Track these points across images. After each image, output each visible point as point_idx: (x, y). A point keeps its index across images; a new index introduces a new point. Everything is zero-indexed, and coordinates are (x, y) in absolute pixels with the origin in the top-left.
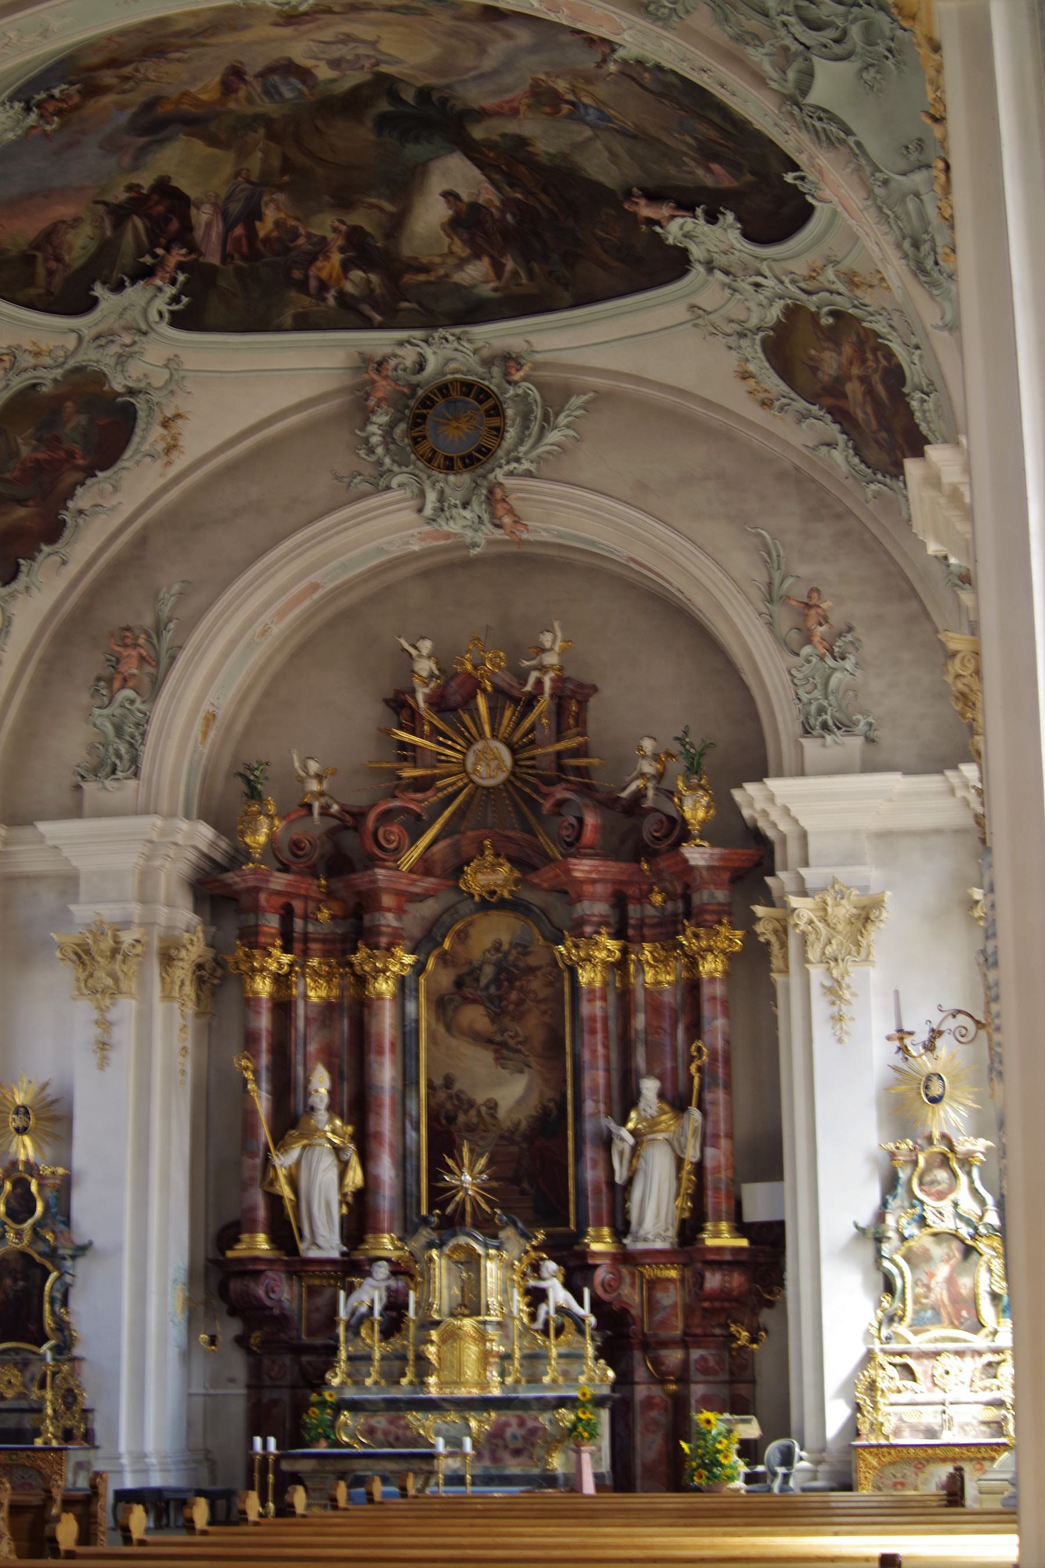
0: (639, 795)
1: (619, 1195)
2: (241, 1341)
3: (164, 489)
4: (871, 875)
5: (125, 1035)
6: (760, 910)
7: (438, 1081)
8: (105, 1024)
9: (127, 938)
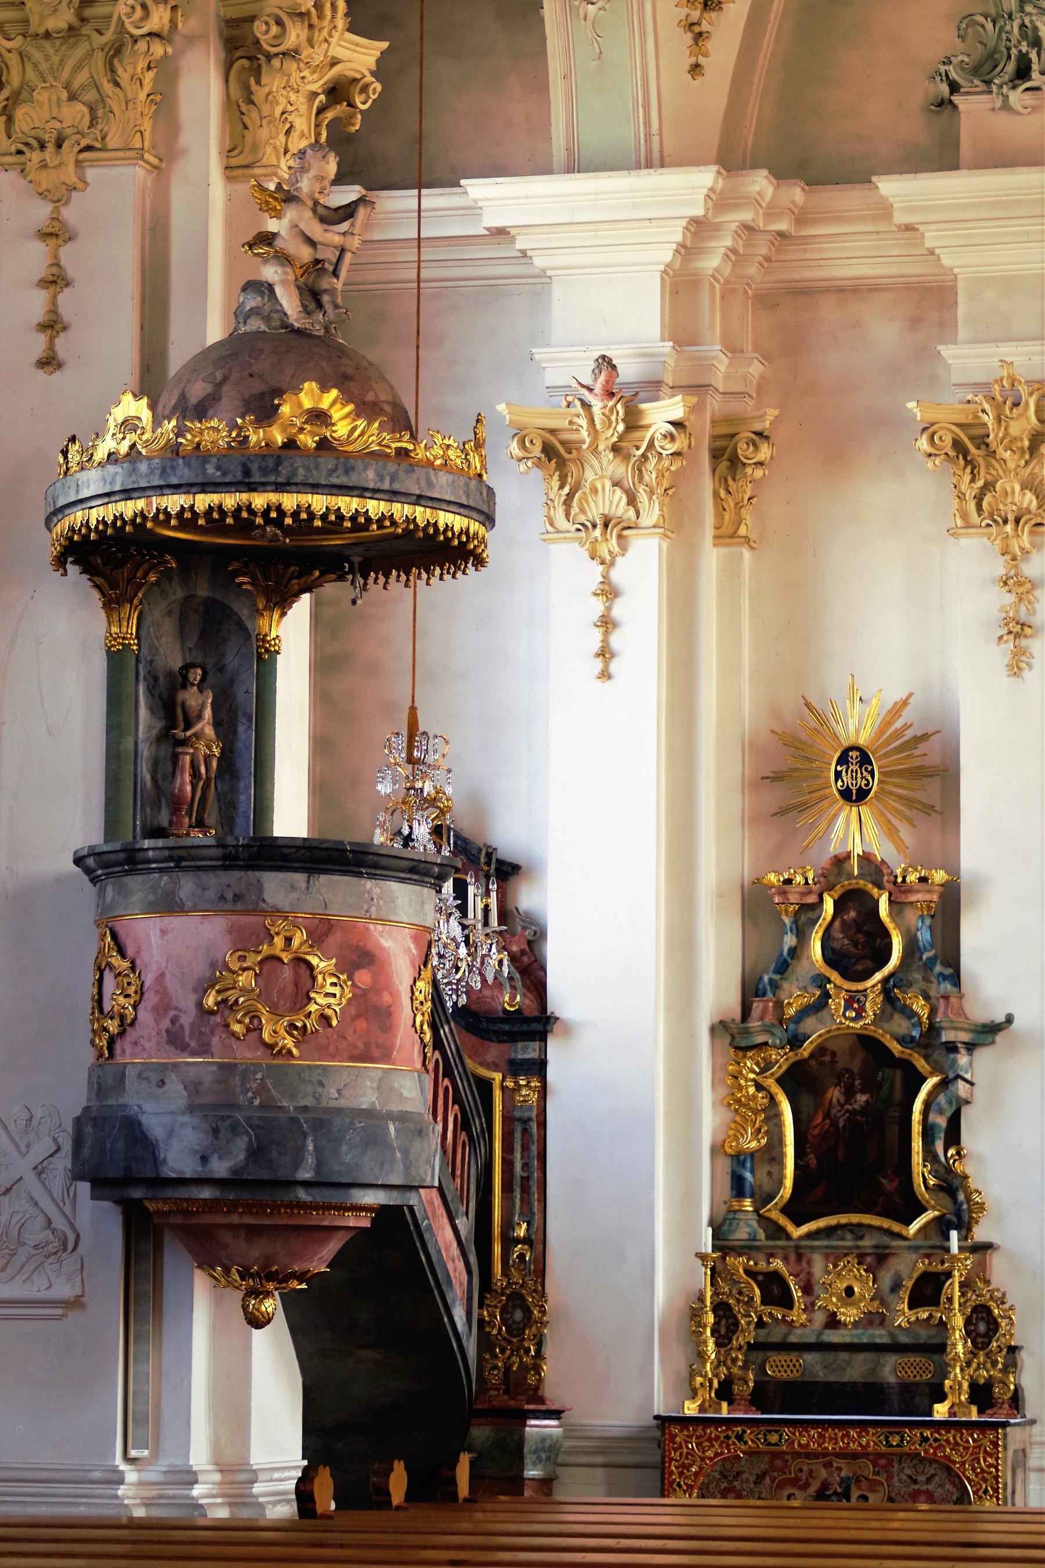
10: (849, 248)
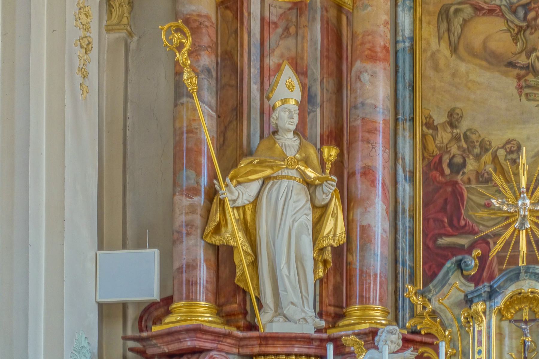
7: (440, 118)
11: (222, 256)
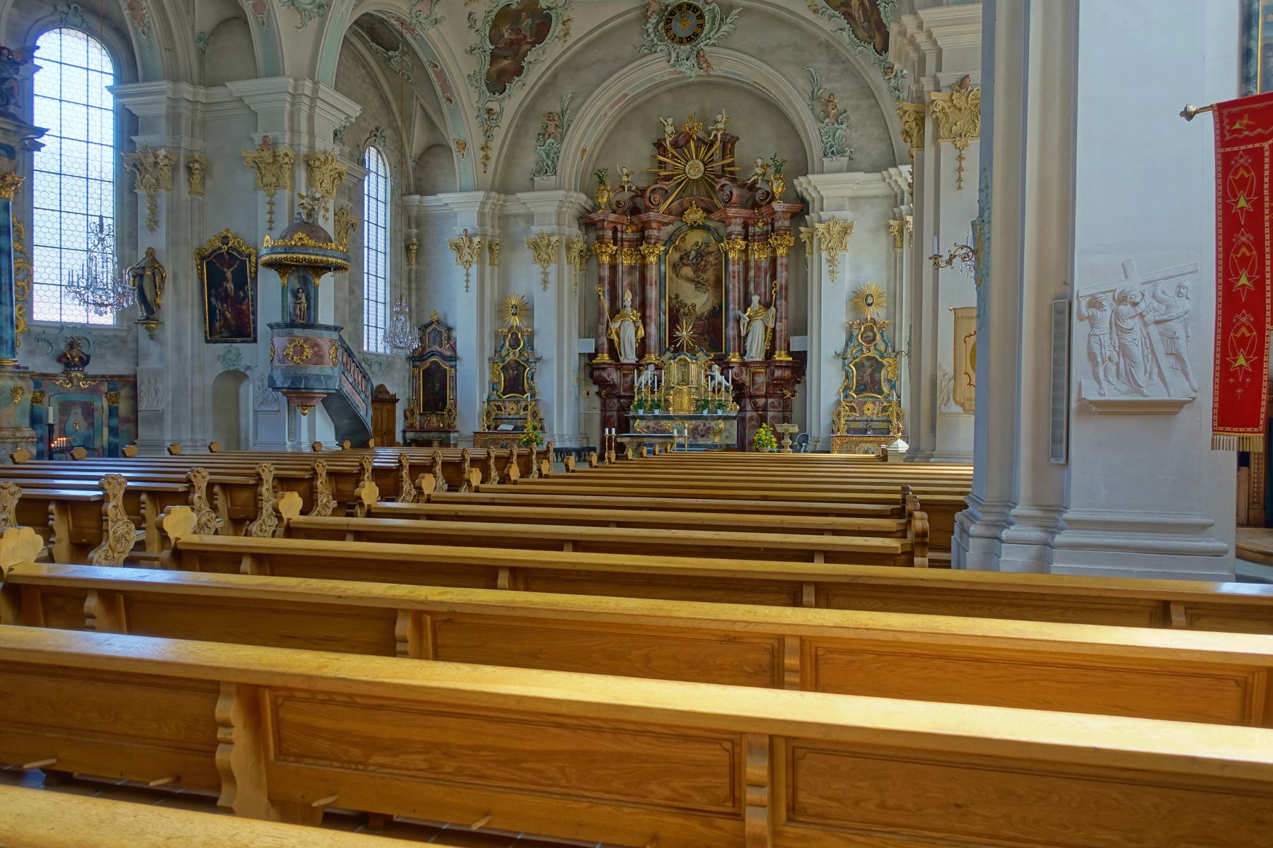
0: (755, 182)
1: (742, 340)
2: (598, 393)
3: (564, 53)
4: (847, 214)
5: (552, 278)
6: (802, 229)
8: (546, 273)
9: (554, 239)
10: (513, 208)
11: (611, 342)
